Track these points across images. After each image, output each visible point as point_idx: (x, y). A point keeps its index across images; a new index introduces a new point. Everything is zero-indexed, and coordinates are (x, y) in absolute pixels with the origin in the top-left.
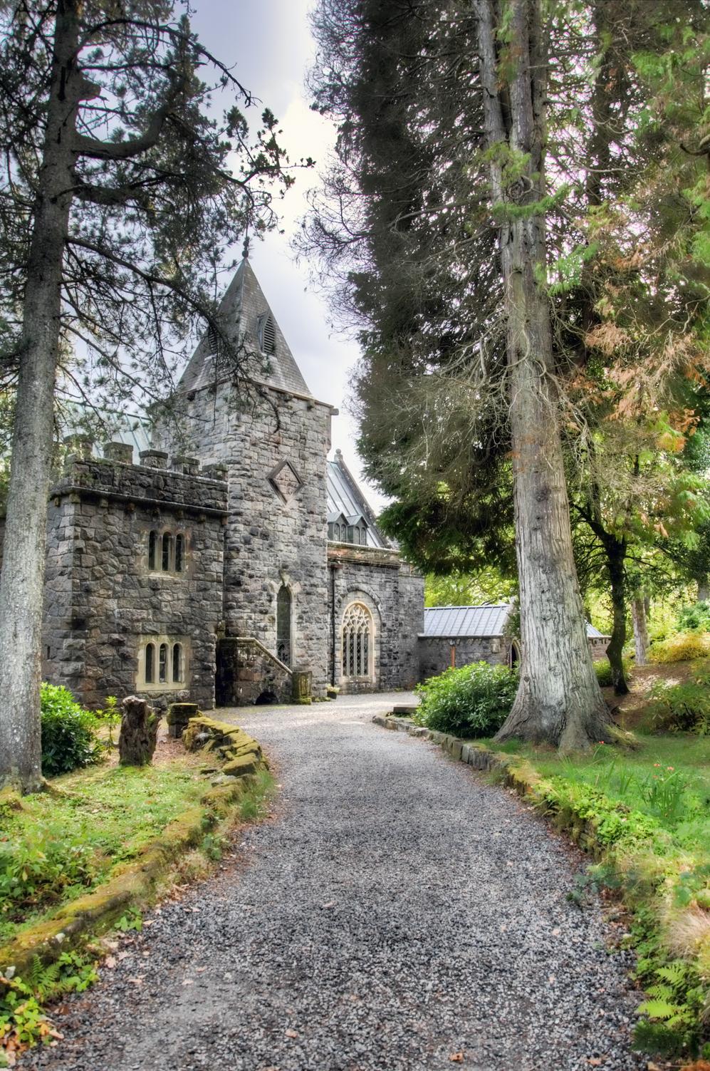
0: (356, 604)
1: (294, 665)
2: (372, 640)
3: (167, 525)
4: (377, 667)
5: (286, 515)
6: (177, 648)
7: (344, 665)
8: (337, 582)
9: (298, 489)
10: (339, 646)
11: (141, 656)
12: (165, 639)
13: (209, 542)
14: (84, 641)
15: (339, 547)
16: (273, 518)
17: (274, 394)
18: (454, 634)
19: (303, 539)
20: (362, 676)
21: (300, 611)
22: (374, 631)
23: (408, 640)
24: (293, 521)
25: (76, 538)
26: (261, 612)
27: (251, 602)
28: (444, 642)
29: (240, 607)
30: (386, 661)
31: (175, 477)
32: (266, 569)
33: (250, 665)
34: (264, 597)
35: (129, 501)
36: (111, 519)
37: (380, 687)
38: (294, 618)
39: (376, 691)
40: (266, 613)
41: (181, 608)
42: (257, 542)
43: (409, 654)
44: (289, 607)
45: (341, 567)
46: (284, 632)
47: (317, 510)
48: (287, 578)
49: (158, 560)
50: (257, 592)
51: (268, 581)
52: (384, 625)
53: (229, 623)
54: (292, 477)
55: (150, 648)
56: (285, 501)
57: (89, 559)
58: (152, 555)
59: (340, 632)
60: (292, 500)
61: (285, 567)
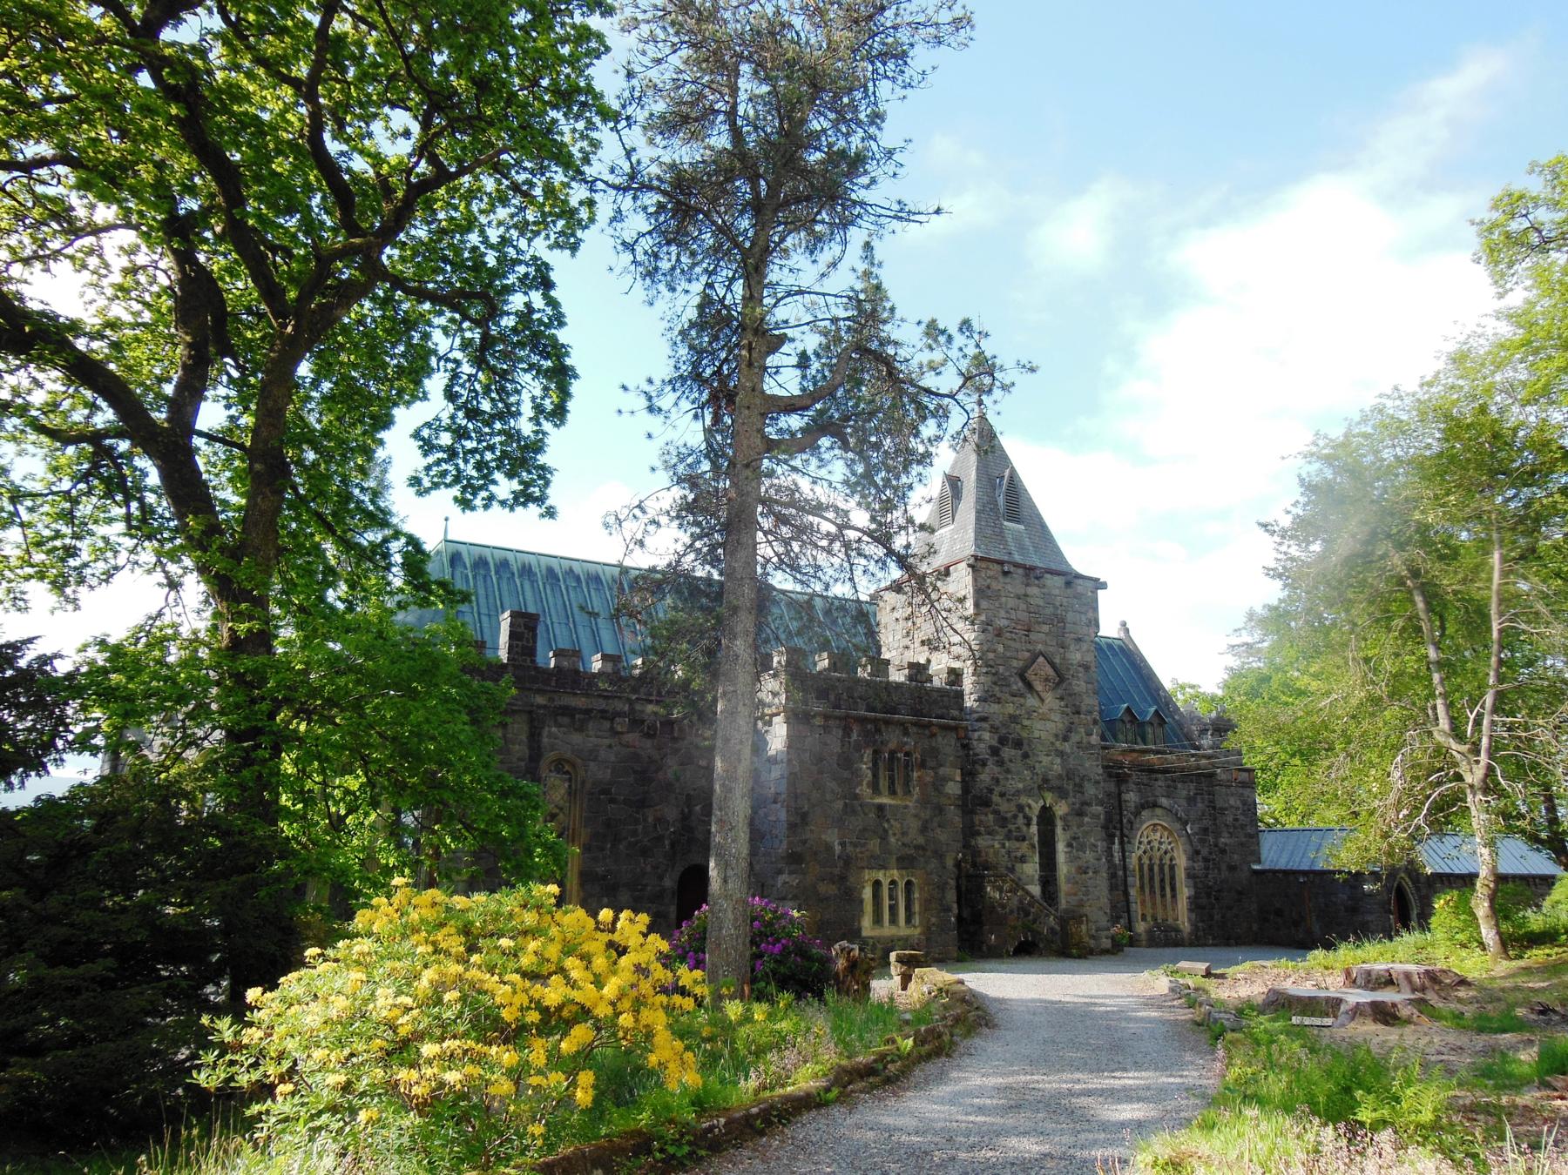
2: (1181, 875)
4: (1190, 910)
5: (1044, 718)
6: (909, 883)
8: (1126, 797)
9: (1058, 685)
11: (867, 893)
12: (895, 874)
16: (1026, 722)
17: (1020, 571)
19: (1067, 747)
22: (1182, 861)
26: (1017, 839)
28: (1291, 878)
30: (1204, 901)
31: (899, 685)
33: (1003, 906)
34: (1021, 820)
38: (1061, 847)
39: (1191, 945)
40: (1024, 839)
42: (1007, 752)
44: (1053, 832)
46: (1048, 863)
47: (1084, 708)
48: (1049, 798)
49: (883, 784)
51: (1024, 800)
52: (1197, 852)
53: (976, 852)
54: (1051, 672)
55: (877, 885)
56: (1042, 700)
58: (875, 776)
59: (1133, 862)
60: (1049, 697)
61: (1045, 780)
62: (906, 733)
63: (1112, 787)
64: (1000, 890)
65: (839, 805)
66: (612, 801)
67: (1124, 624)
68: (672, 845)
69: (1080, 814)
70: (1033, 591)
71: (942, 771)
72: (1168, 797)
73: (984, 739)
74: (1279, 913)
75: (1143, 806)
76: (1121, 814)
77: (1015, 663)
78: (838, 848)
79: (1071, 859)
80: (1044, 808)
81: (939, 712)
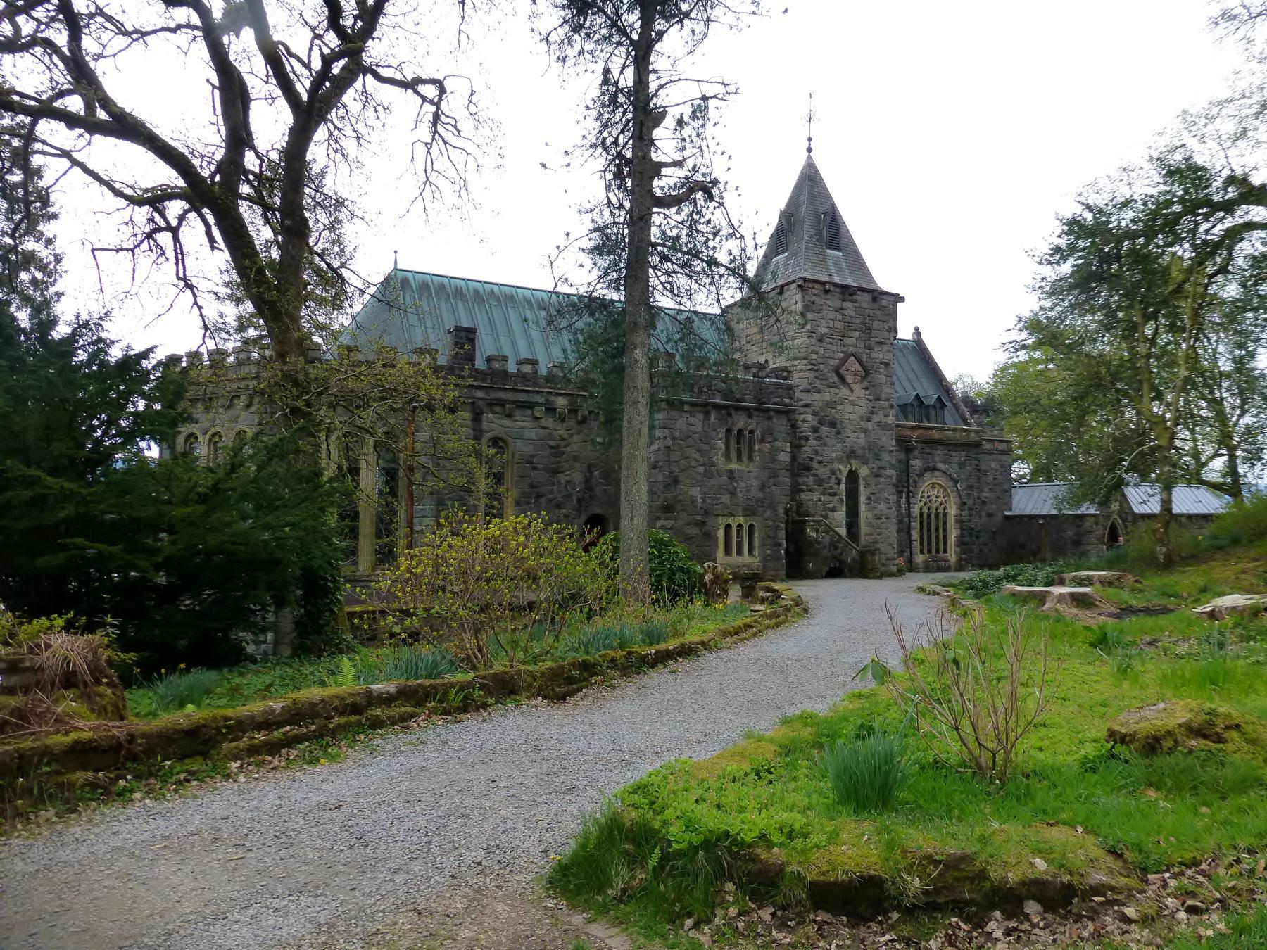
1: (863, 541)
2: (951, 521)
3: (741, 421)
4: (957, 546)
6: (751, 526)
7: (922, 544)
8: (912, 463)
9: (864, 378)
10: (916, 525)
11: (721, 534)
12: (741, 519)
13: (777, 435)
15: (913, 428)
16: (839, 407)
17: (838, 290)
19: (869, 425)
20: (941, 554)
21: (869, 490)
22: (953, 511)
25: (665, 438)
26: (830, 494)
27: (820, 485)
30: (967, 539)
32: (834, 455)
33: (819, 543)
34: (833, 480)
35: (705, 405)
36: (693, 421)
40: (835, 494)
41: (756, 493)
42: (825, 430)
44: (857, 489)
45: (916, 447)
46: (853, 512)
47: (883, 396)
49: (734, 454)
51: (836, 466)
52: (964, 503)
53: (800, 505)
54: (859, 368)
55: (728, 527)
56: (852, 390)
57: (675, 456)
58: (727, 448)
59: (916, 511)
60: (857, 388)
61: (853, 452)
62: (750, 416)
63: (902, 456)
64: (817, 531)
65: (701, 469)
66: (535, 468)
67: (917, 329)
68: (579, 500)
70: (848, 305)
71: (778, 444)
73: (807, 421)
74: (1022, 547)
75: (925, 470)
76: (908, 476)
77: (832, 362)
80: (851, 471)
81: (776, 400)
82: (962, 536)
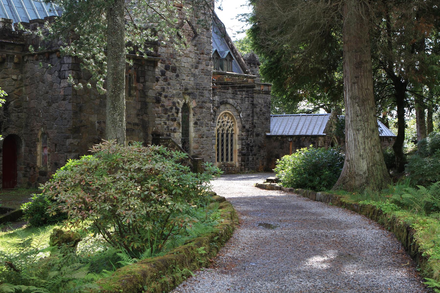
0: (226, 113)
2: (236, 137)
7: (218, 155)
9: (194, 38)
14: (79, 140)
16: (178, 58)
18: (291, 133)
19: (197, 72)
22: (237, 131)
23: (260, 137)
24: (190, 60)
27: (166, 114)
28: (285, 139)
29: (159, 117)
34: (174, 111)
37: (241, 170)
38: (192, 124)
42: (169, 74)
43: (260, 147)
44: (188, 116)
46: (186, 133)
47: (205, 52)
48: (187, 97)
50: (169, 107)
51: (176, 100)
60: (189, 44)
61: (186, 89)
69: (201, 108)
72: (232, 98)
78: (97, 125)
79: (197, 131)
82: (242, 149)
